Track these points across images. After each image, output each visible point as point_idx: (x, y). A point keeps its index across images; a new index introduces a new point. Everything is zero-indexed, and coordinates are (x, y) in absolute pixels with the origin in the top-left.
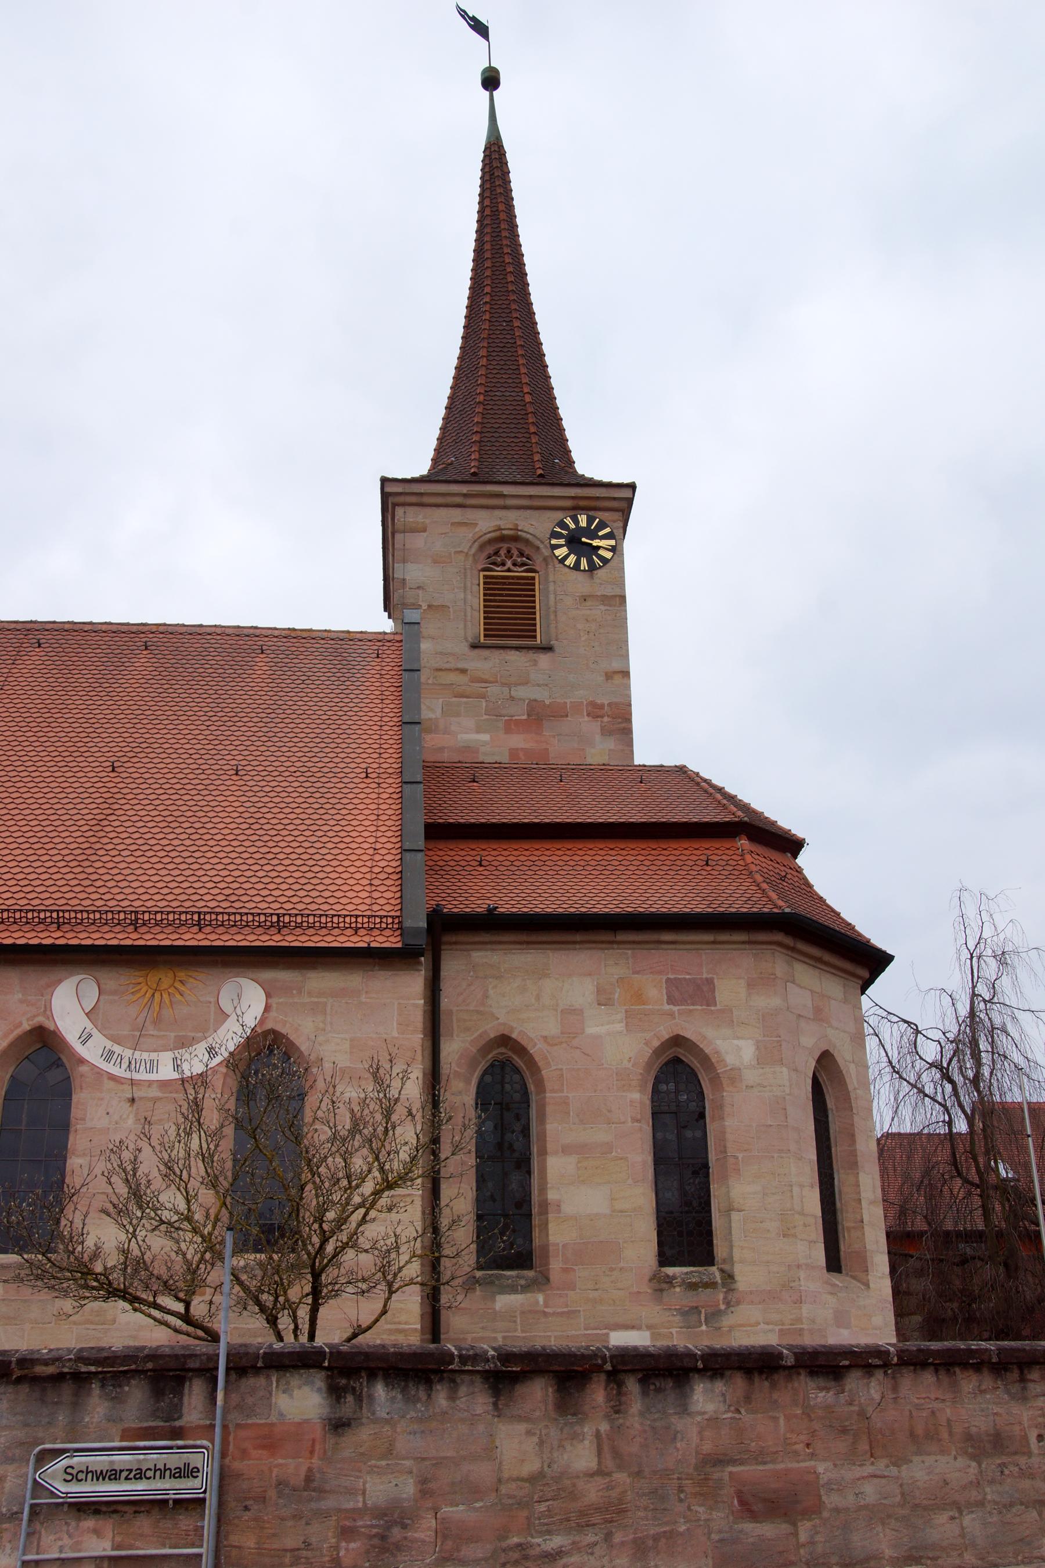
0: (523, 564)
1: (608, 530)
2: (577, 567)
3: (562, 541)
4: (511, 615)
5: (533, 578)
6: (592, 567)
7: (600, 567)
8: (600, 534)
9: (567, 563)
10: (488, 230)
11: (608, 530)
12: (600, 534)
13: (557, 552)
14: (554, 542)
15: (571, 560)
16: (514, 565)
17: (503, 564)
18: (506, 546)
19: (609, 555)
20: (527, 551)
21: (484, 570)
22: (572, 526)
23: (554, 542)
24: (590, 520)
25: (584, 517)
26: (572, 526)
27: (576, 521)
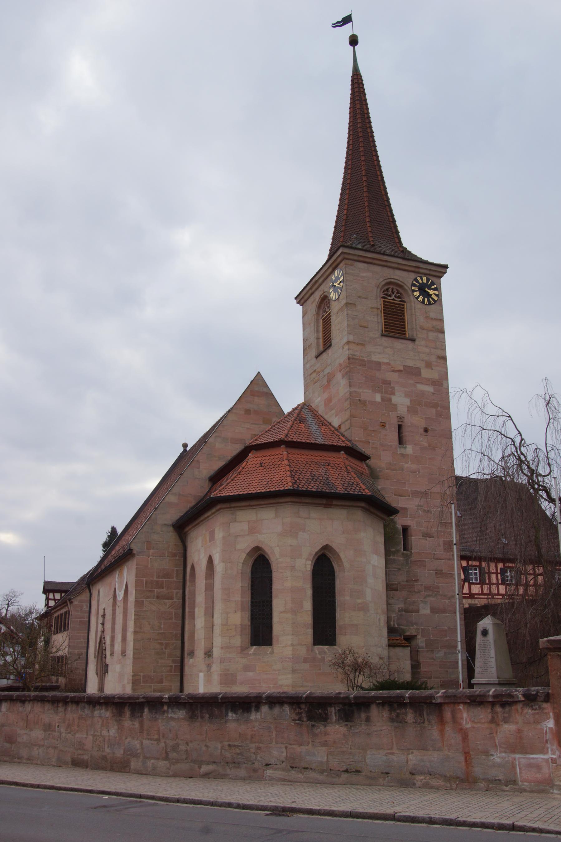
0: (399, 297)
1: (435, 286)
2: (423, 302)
3: (416, 289)
4: (395, 323)
5: (403, 305)
6: (430, 304)
7: (433, 304)
8: (432, 287)
9: (419, 299)
10: (366, 116)
11: (435, 286)
12: (432, 287)
13: (415, 294)
14: (413, 288)
15: (421, 298)
16: (395, 296)
17: (390, 296)
18: (391, 286)
19: (436, 298)
20: (401, 291)
21: (383, 298)
22: (421, 282)
23: (413, 288)
24: (428, 280)
25: (425, 278)
26: (421, 282)
27: (422, 280)
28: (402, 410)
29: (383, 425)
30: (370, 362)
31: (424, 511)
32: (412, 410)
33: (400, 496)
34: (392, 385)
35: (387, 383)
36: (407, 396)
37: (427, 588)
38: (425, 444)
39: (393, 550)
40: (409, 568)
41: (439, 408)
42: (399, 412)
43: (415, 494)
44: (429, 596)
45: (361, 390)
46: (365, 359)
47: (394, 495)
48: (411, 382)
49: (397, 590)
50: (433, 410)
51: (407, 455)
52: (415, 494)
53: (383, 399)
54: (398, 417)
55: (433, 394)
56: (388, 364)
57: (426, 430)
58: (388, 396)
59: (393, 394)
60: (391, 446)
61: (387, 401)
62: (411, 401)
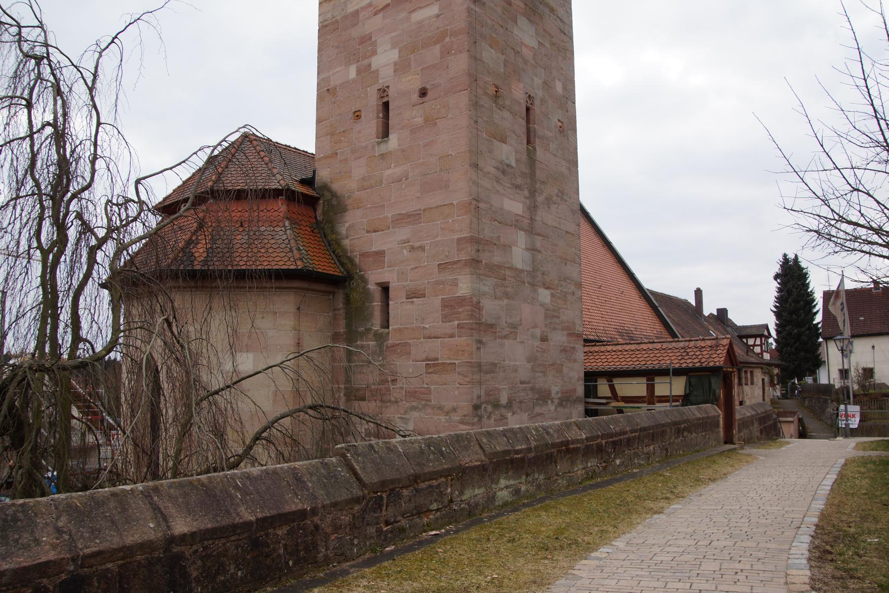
28: (386, 76)
29: (357, 115)
30: (345, 17)
31: (413, 248)
32: (401, 67)
33: (375, 231)
34: (373, 39)
35: (366, 39)
36: (393, 47)
37: (412, 394)
38: (419, 120)
39: (361, 329)
40: (383, 359)
41: (447, 39)
42: (380, 81)
43: (403, 219)
44: (414, 408)
45: (331, 73)
46: (338, 18)
47: (368, 232)
48: (403, 15)
49: (363, 399)
50: (437, 49)
51: (390, 153)
52: (403, 219)
53: (359, 72)
54: (379, 90)
55: (438, 16)
56: (370, 5)
57: (423, 93)
58: (366, 62)
59: (374, 53)
60: (366, 147)
61: (366, 72)
62: (400, 52)
